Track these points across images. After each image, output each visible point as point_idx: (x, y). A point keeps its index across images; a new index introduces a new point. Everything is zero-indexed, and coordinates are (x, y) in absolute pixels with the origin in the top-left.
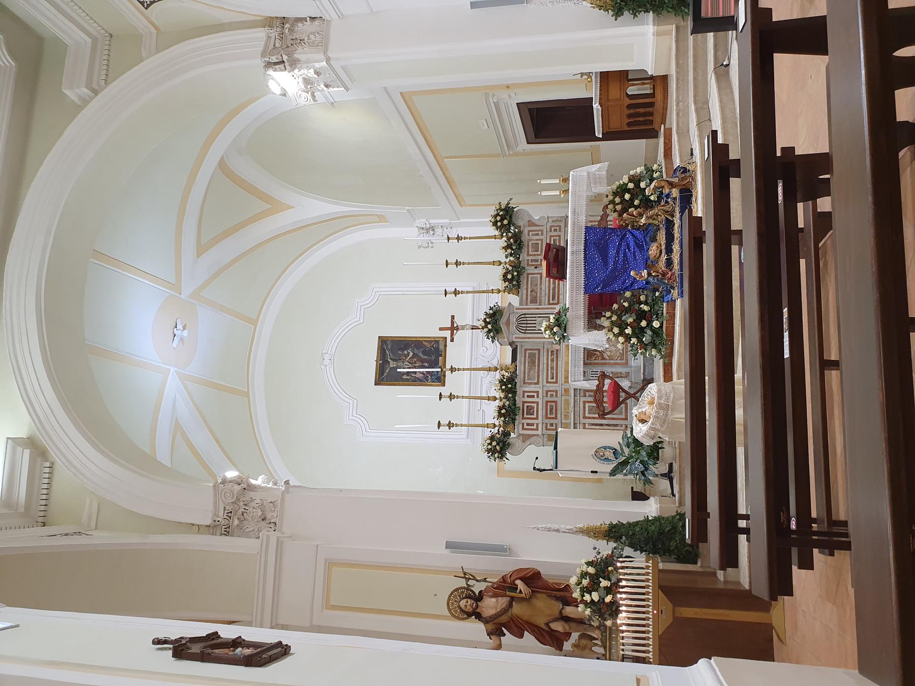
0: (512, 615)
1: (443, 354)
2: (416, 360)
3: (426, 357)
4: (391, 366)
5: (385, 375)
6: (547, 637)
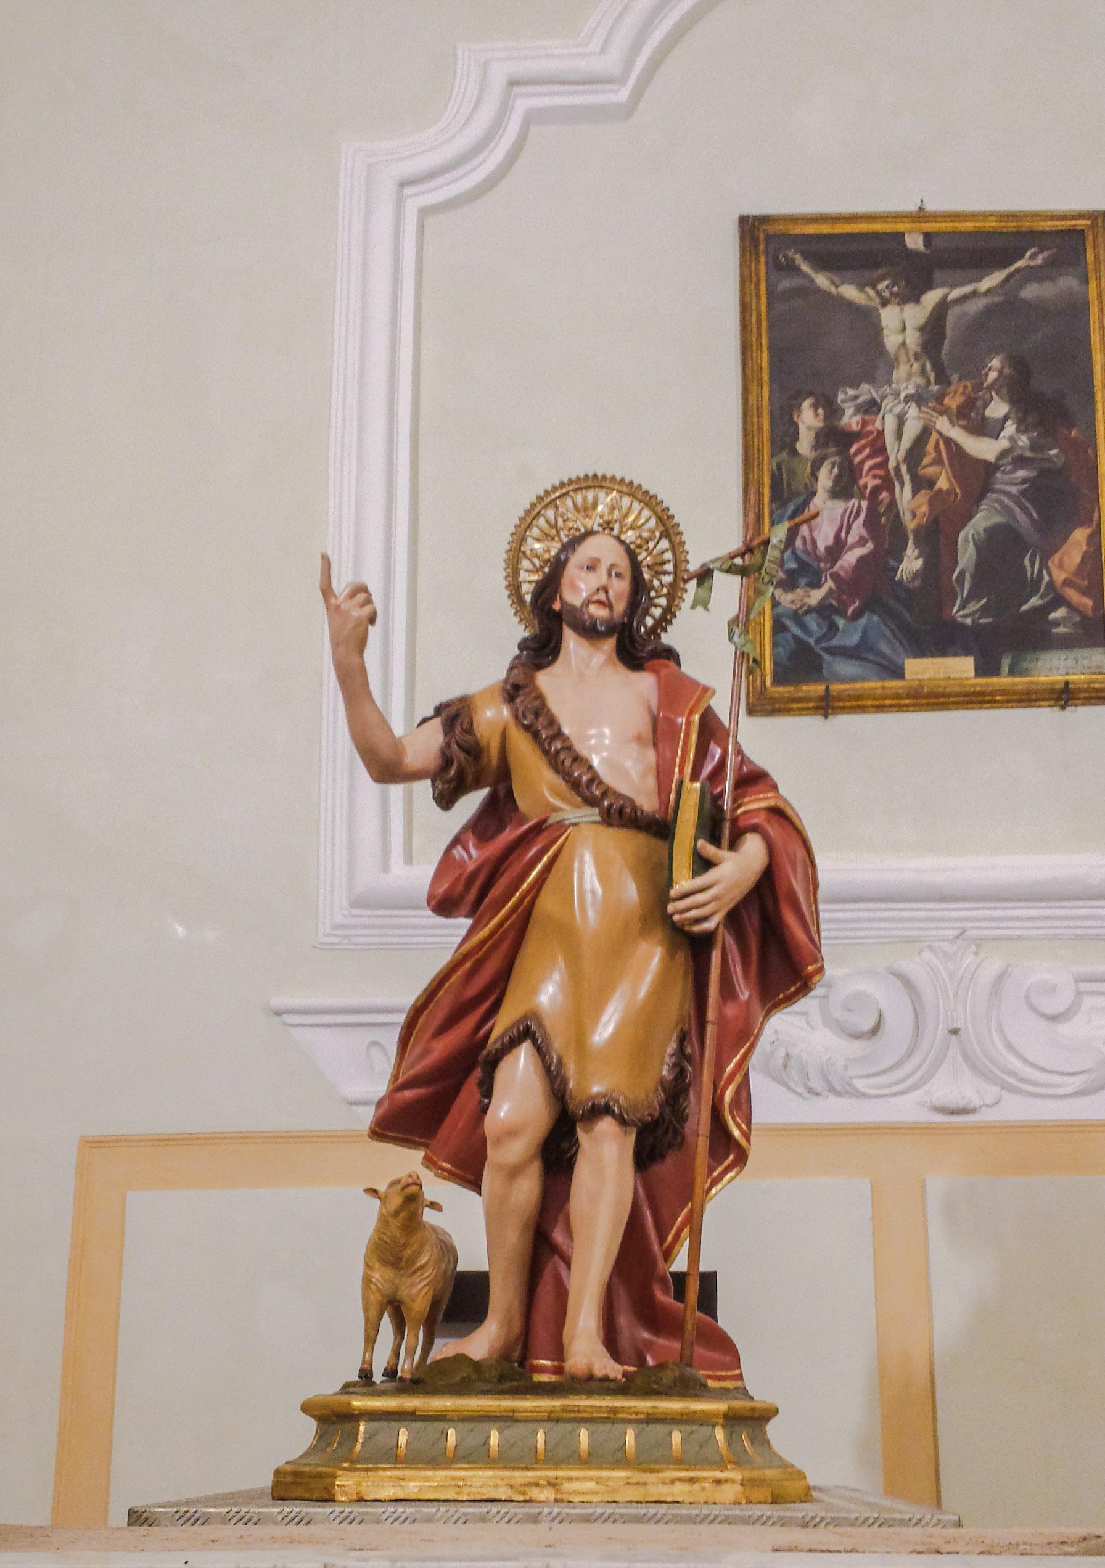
0: (561, 827)
1: (1003, 681)
2: (943, 484)
3: (967, 556)
4: (889, 317)
5: (822, 280)
6: (441, 1048)
